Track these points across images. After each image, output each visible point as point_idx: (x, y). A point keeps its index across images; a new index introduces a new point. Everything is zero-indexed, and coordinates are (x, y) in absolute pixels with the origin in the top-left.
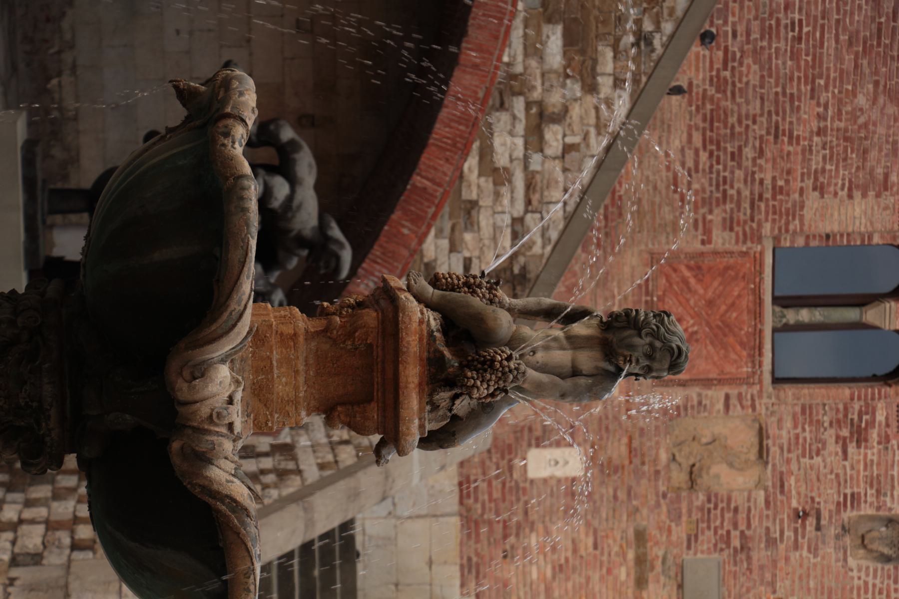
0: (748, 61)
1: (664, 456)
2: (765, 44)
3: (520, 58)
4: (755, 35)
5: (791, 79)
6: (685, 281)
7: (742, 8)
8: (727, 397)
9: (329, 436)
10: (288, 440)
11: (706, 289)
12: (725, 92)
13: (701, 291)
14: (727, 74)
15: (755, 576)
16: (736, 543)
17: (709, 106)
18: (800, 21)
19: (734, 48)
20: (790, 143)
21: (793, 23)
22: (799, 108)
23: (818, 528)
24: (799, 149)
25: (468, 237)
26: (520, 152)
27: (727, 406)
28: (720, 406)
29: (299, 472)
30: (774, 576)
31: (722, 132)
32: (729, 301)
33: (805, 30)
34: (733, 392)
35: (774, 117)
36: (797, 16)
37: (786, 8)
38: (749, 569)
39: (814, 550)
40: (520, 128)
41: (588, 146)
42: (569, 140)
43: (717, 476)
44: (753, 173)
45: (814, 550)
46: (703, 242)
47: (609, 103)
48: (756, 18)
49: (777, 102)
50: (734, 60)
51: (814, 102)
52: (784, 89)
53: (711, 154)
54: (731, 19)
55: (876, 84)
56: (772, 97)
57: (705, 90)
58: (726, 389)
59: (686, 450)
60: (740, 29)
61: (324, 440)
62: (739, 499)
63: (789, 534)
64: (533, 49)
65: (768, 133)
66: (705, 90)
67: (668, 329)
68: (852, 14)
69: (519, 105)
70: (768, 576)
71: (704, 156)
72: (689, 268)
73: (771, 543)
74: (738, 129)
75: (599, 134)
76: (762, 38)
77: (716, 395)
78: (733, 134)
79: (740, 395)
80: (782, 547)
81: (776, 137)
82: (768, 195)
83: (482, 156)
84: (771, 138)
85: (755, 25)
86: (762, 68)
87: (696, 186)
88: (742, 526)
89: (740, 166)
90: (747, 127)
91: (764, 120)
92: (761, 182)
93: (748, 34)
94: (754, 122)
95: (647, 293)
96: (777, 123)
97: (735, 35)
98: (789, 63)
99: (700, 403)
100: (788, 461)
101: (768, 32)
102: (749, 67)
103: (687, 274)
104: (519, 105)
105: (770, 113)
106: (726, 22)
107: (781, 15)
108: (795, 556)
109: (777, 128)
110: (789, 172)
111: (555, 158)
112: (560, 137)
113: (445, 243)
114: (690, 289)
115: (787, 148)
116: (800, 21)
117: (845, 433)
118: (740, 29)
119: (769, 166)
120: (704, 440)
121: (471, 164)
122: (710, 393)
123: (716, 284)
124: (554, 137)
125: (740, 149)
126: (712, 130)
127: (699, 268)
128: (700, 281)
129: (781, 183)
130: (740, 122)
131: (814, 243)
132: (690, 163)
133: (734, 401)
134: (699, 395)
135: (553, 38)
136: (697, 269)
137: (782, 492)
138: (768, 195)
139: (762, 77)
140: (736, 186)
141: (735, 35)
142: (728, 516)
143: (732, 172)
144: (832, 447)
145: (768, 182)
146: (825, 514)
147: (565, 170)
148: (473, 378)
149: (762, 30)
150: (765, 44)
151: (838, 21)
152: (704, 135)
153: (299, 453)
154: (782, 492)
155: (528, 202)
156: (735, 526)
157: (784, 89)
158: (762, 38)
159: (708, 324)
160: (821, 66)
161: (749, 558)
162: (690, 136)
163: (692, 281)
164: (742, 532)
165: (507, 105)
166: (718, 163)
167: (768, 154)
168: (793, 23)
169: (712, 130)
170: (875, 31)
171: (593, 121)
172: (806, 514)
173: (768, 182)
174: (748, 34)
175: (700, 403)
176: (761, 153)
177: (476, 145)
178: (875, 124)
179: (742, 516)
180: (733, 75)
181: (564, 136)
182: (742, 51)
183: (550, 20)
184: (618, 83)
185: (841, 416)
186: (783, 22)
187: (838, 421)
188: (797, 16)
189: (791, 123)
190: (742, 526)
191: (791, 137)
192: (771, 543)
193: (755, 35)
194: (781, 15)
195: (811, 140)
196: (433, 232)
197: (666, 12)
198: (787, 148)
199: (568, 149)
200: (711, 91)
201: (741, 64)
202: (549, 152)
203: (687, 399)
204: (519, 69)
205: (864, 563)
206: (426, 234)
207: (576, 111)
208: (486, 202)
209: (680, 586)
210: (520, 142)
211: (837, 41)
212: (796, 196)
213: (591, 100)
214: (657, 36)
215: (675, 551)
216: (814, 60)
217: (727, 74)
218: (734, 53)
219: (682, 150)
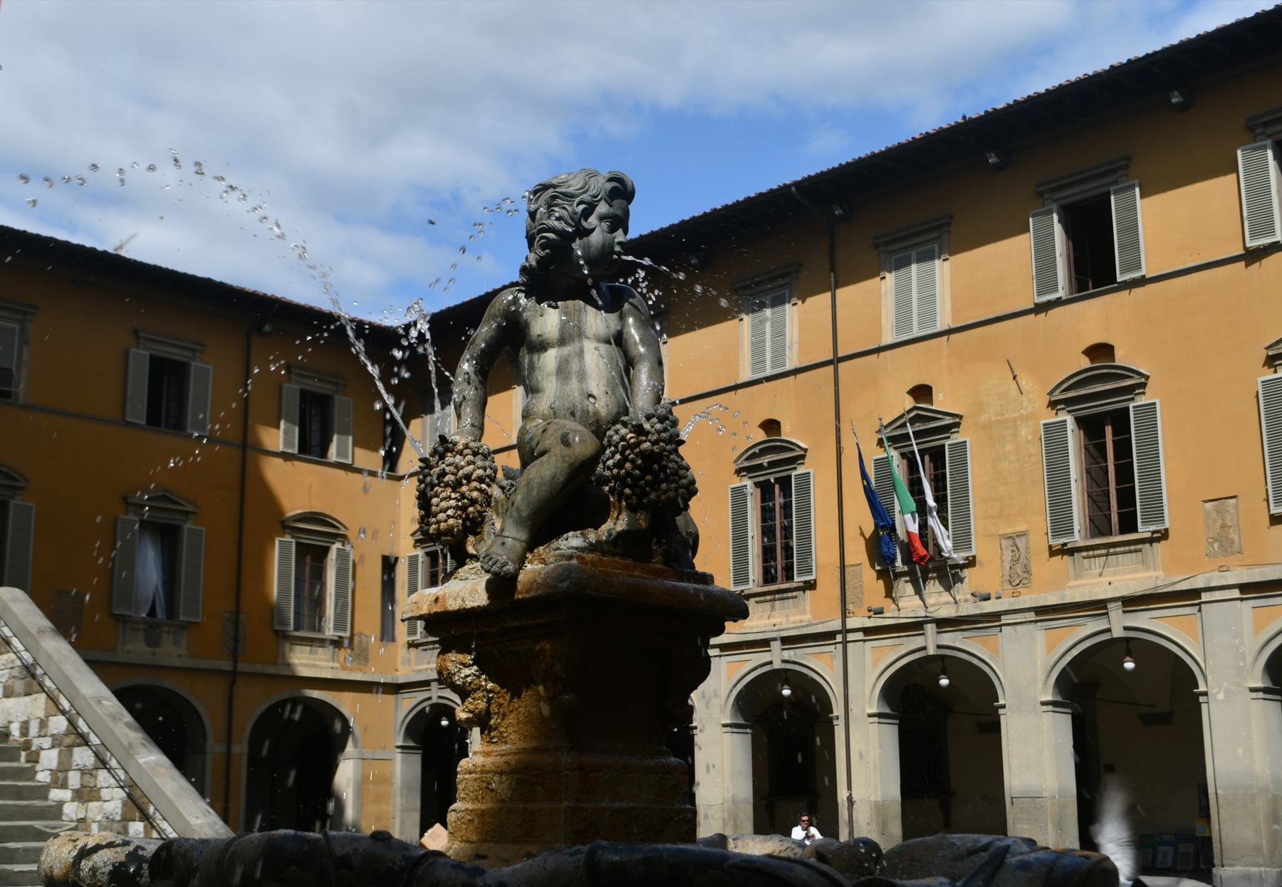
67: (581, 189)
148: (676, 490)
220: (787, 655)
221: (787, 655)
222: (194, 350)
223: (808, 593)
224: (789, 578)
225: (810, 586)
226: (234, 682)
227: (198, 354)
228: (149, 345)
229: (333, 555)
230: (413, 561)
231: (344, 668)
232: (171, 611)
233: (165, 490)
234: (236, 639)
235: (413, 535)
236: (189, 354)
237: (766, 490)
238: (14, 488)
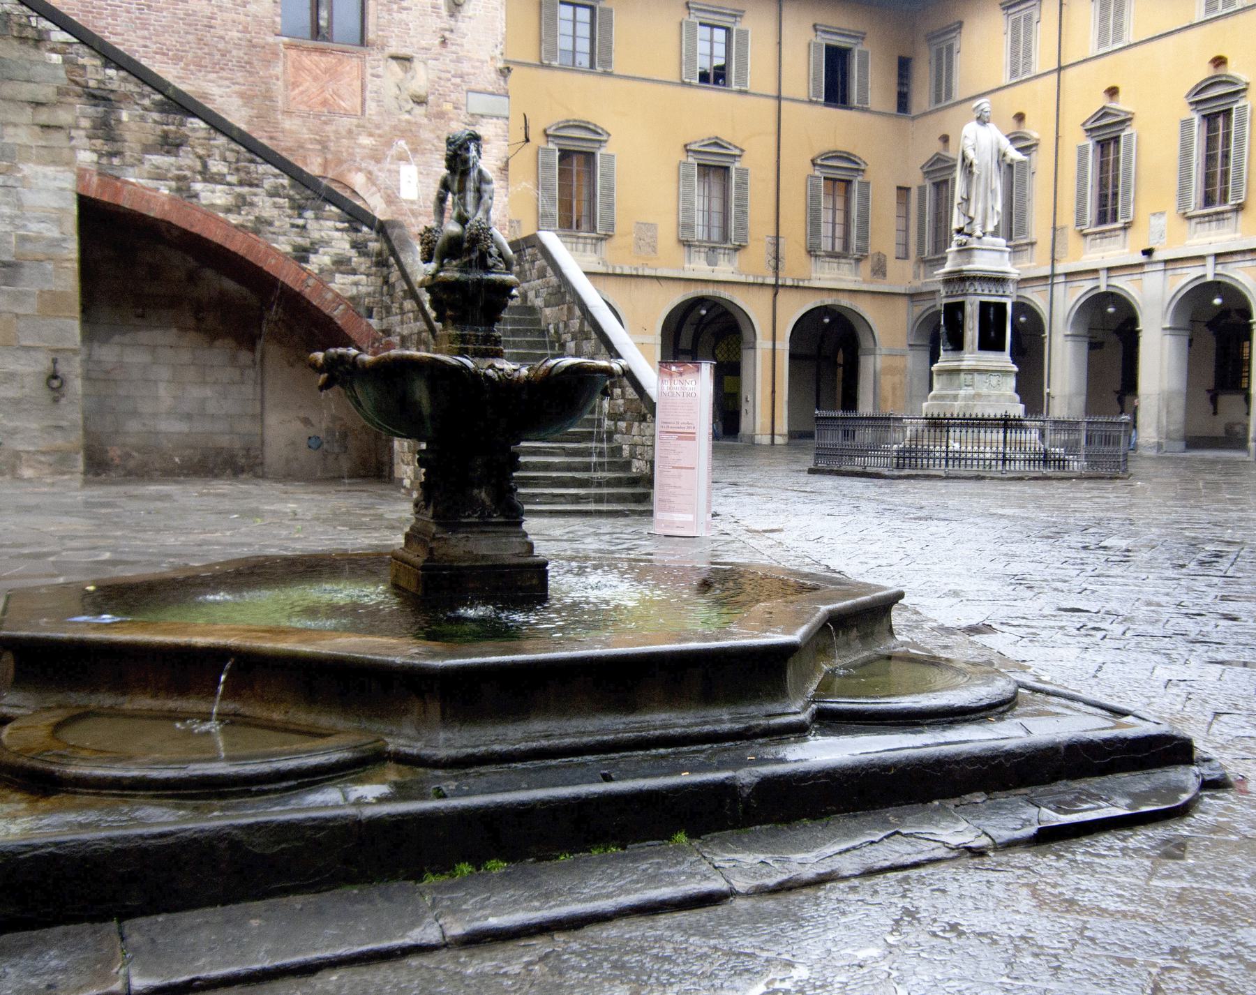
0: (162, 39)
1: (407, 117)
2: (151, 28)
4: (146, 33)
6: (302, 93)
7: (128, 40)
8: (373, 75)
9: (396, 314)
10: (398, 338)
11: (307, 80)
12: (182, 57)
13: (308, 84)
14: (170, 53)
15: (477, 71)
16: (458, 80)
18: (137, 4)
19: (154, 47)
20: (216, 19)
21: (139, 9)
23: (452, 31)
24: (219, 13)
25: (277, 223)
27: (378, 76)
28: (378, 81)
29: (419, 333)
30: (478, 60)
32: (314, 67)
34: (369, 71)
35: (199, 27)
36: (134, 6)
37: (129, 12)
38: (474, 74)
39: (464, 36)
43: (420, 86)
44: (235, 44)
45: (464, 36)
46: (278, 79)
47: (194, 130)
48: (135, 32)
49: (190, 25)
50: (162, 49)
52: (181, 19)
53: (222, 69)
54: (135, 48)
57: (182, 69)
58: (368, 78)
59: (403, 103)
60: (141, 42)
61: (399, 317)
62: (432, 76)
63: (454, 48)
65: (209, 32)
66: (182, 69)
70: (478, 64)
71: (224, 74)
72: (293, 89)
73: (459, 60)
74: (206, 50)
75: (214, 139)
76: (148, 29)
77: (372, 84)
78: (209, 54)
79: (373, 68)
80: (461, 54)
81: (211, 27)
82: (248, 36)
83: (228, 210)
84: (212, 30)
85: (140, 33)
86: (167, 32)
87: (241, 80)
88: (449, 76)
89: (230, 52)
91: (200, 33)
92: (240, 39)
93: (146, 38)
95: (308, 117)
97: (145, 46)
98: (165, 14)
99: (376, 92)
100: (412, 43)
101: (144, 26)
103: (297, 91)
105: (196, 30)
107: (133, 16)
108: (467, 46)
109: (206, 26)
110: (234, 22)
113: (282, 238)
114: (306, 91)
115: (219, 21)
116: (137, 4)
117: (395, 7)
118: (141, 42)
119: (229, 33)
120: (398, 92)
121: (234, 219)
122: (369, 86)
123: (304, 75)
124: (216, 166)
125: (219, 50)
126: (206, 67)
127: (293, 83)
128: (301, 84)
129: (240, 27)
130: (201, 49)
131: (279, 11)
132: (227, 83)
133: (374, 71)
134: (371, 92)
135: (154, 162)
136: (295, 85)
137: (430, 50)
138: (248, 36)
139: (173, 32)
140: (242, 55)
142: (442, 83)
143: (233, 57)
144: (404, 15)
145: (239, 35)
146: (443, 25)
150: (151, 28)
152: (209, 72)
153: (405, 332)
154: (430, 50)
155: (257, 186)
156: (449, 80)
157: (181, 19)
158: (148, 29)
159: (328, 82)
161: (468, 74)
162: (210, 81)
163: (301, 88)
164: (453, 76)
166: (227, 65)
167: (222, 33)
168: (139, 9)
169: (206, 67)
172: (443, 37)
173: (239, 35)
174: (146, 38)
175: (376, 92)
176: (222, 38)
177: (221, 215)
179: (444, 75)
180: (172, 50)
182: (156, 43)
185: (385, 8)
186: (138, 15)
187: (389, 10)
188: (134, 6)
189: (203, 16)
190: (449, 76)
191: (212, 18)
192: (459, 60)
193: (146, 33)
195: (213, 5)
196: (275, 245)
197: (139, 90)
198: (219, 21)
200: (182, 64)
203: (373, 99)
205: (471, 6)
206: (275, 249)
207: (201, 151)
208: (257, 212)
209: (482, 116)
210: (219, 187)
212: (249, 18)
215: (462, 117)
217: (170, 53)
218: (157, 48)
220: (1219, 269)
221: (1219, 269)
222: (735, 16)
223: (1241, 215)
224: (1225, 201)
225: (1239, 208)
226: (775, 295)
227: (738, 19)
228: (698, 14)
229: (855, 186)
230: (922, 189)
231: (864, 281)
232: (725, 237)
233: (717, 138)
234: (777, 258)
235: (921, 168)
236: (732, 20)
237: (1210, 119)
238: (600, 141)
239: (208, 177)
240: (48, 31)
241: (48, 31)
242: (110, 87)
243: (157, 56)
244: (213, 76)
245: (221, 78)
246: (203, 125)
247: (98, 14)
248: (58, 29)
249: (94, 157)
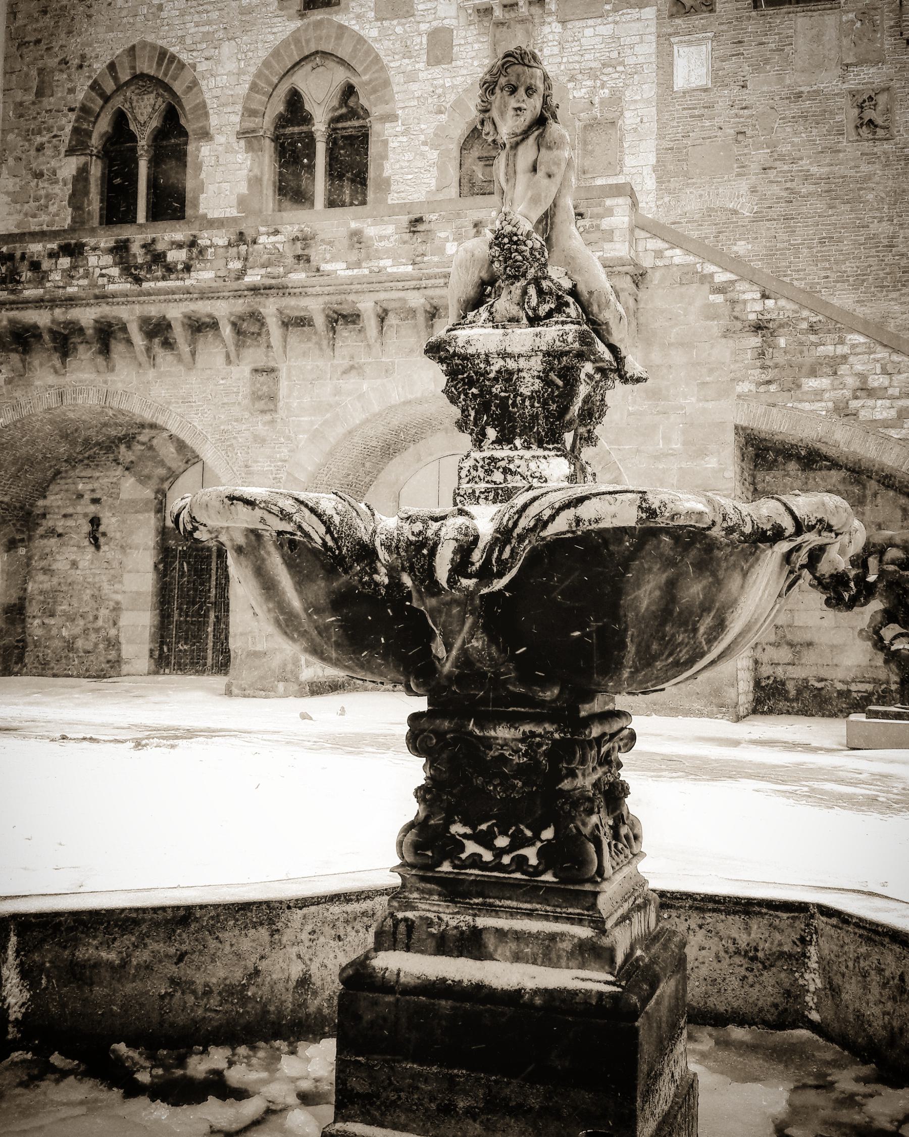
3: (824, 404)
5: (855, 240)
17: (873, 289)
22: (874, 235)
26: (887, 403)
31: (889, 279)
33: (824, 235)
40: (870, 402)
41: (883, 358)
42: (878, 371)
47: (853, 346)
51: (871, 225)
54: (816, 281)
55: (860, 189)
56: (867, 251)
64: (818, 395)
65: (891, 251)
68: (816, 208)
69: (854, 404)
90: (886, 265)
93: (826, 269)
94: (883, 260)
96: (883, 246)
102: (846, 267)
104: (854, 404)
106: (818, 283)
109: (887, 246)
111: (891, 379)
112: (876, 377)
115: (901, 239)
124: (876, 381)
141: (827, 277)
147: (899, 372)
149: (823, 261)
151: (819, 216)
160: (847, 224)
165: (854, 412)
170: (826, 194)
171: (866, 356)
174: (826, 269)
178: (886, 187)
181: (875, 374)
183: (799, 386)
184: (842, 342)
194: (815, 251)
198: (901, 239)
199: (884, 372)
201: (845, 272)
202: (886, 383)
204: (831, 405)
207: (859, 368)
210: (879, 402)
211: (830, 216)
213: (851, 359)
214: (811, 319)
216: (844, 228)
217: (851, 279)
219: (901, 304)
239: (865, 390)
240: (712, 275)
241: (712, 275)
242: (769, 317)
243: (838, 285)
244: (894, 295)
245: (901, 295)
246: (862, 339)
247: (781, 254)
248: (720, 270)
249: (753, 387)
